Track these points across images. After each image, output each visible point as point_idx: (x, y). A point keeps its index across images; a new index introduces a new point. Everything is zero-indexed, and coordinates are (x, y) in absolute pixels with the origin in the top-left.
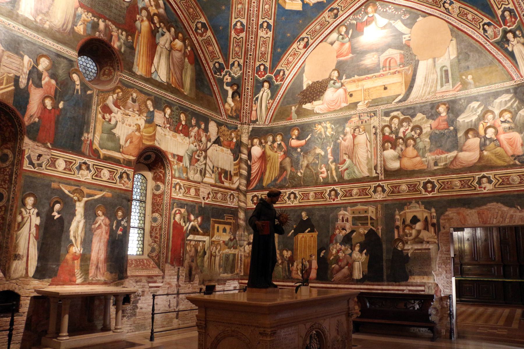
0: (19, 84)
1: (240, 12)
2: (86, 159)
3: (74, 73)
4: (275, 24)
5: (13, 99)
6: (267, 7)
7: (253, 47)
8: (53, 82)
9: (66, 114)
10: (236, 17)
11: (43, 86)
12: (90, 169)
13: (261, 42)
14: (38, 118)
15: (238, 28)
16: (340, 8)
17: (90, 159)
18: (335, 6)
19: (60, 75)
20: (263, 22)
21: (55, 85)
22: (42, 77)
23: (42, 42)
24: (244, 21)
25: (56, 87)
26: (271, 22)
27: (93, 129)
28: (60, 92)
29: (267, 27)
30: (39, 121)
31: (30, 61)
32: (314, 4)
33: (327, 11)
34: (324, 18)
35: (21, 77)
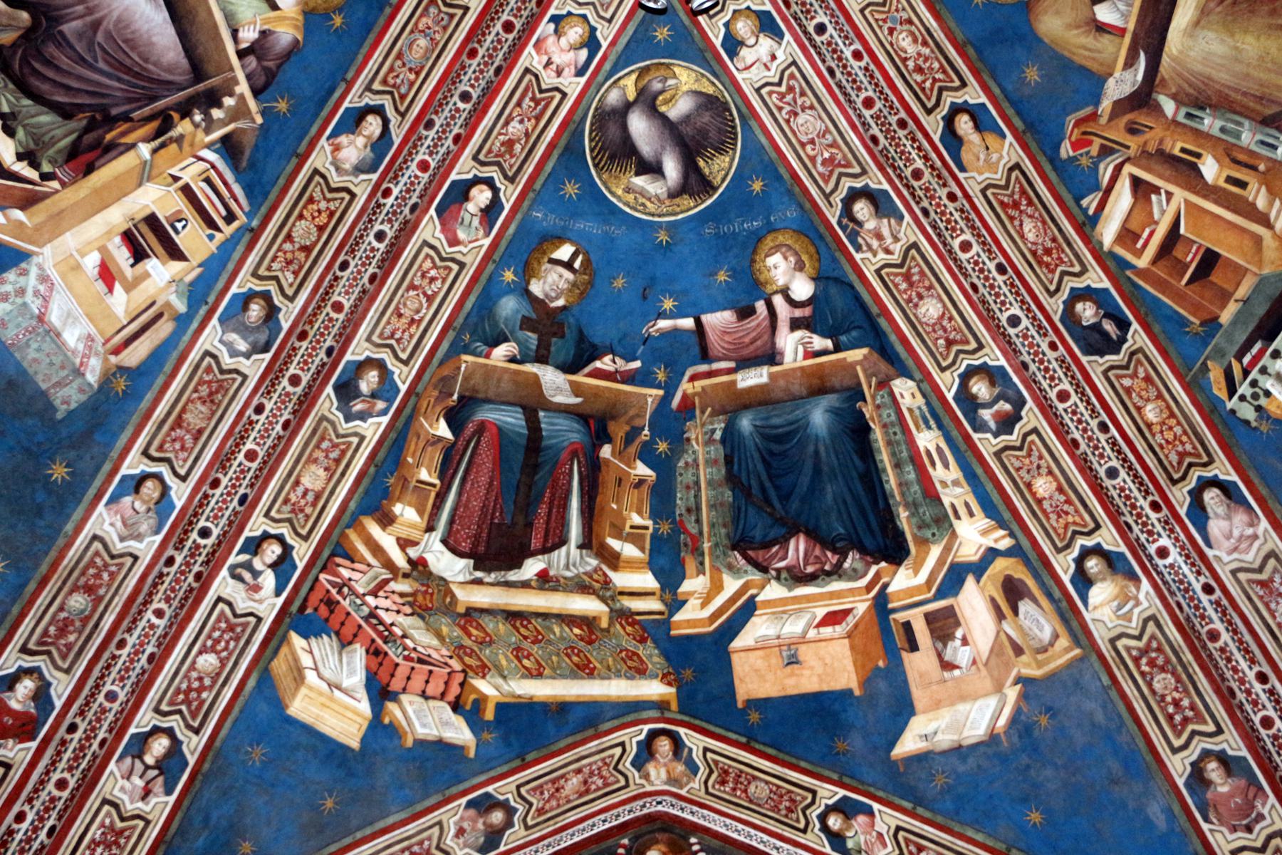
1: (63, 631)
4: (206, 766)
6: (208, 662)
7: (43, 835)
10: (31, 646)
13: (95, 832)
15: (14, 705)
16: (521, 809)
18: (504, 789)
20: (156, 730)
24: (61, 688)
26: (192, 746)
29: (160, 765)
32: (420, 743)
33: (464, 801)
34: (436, 830)
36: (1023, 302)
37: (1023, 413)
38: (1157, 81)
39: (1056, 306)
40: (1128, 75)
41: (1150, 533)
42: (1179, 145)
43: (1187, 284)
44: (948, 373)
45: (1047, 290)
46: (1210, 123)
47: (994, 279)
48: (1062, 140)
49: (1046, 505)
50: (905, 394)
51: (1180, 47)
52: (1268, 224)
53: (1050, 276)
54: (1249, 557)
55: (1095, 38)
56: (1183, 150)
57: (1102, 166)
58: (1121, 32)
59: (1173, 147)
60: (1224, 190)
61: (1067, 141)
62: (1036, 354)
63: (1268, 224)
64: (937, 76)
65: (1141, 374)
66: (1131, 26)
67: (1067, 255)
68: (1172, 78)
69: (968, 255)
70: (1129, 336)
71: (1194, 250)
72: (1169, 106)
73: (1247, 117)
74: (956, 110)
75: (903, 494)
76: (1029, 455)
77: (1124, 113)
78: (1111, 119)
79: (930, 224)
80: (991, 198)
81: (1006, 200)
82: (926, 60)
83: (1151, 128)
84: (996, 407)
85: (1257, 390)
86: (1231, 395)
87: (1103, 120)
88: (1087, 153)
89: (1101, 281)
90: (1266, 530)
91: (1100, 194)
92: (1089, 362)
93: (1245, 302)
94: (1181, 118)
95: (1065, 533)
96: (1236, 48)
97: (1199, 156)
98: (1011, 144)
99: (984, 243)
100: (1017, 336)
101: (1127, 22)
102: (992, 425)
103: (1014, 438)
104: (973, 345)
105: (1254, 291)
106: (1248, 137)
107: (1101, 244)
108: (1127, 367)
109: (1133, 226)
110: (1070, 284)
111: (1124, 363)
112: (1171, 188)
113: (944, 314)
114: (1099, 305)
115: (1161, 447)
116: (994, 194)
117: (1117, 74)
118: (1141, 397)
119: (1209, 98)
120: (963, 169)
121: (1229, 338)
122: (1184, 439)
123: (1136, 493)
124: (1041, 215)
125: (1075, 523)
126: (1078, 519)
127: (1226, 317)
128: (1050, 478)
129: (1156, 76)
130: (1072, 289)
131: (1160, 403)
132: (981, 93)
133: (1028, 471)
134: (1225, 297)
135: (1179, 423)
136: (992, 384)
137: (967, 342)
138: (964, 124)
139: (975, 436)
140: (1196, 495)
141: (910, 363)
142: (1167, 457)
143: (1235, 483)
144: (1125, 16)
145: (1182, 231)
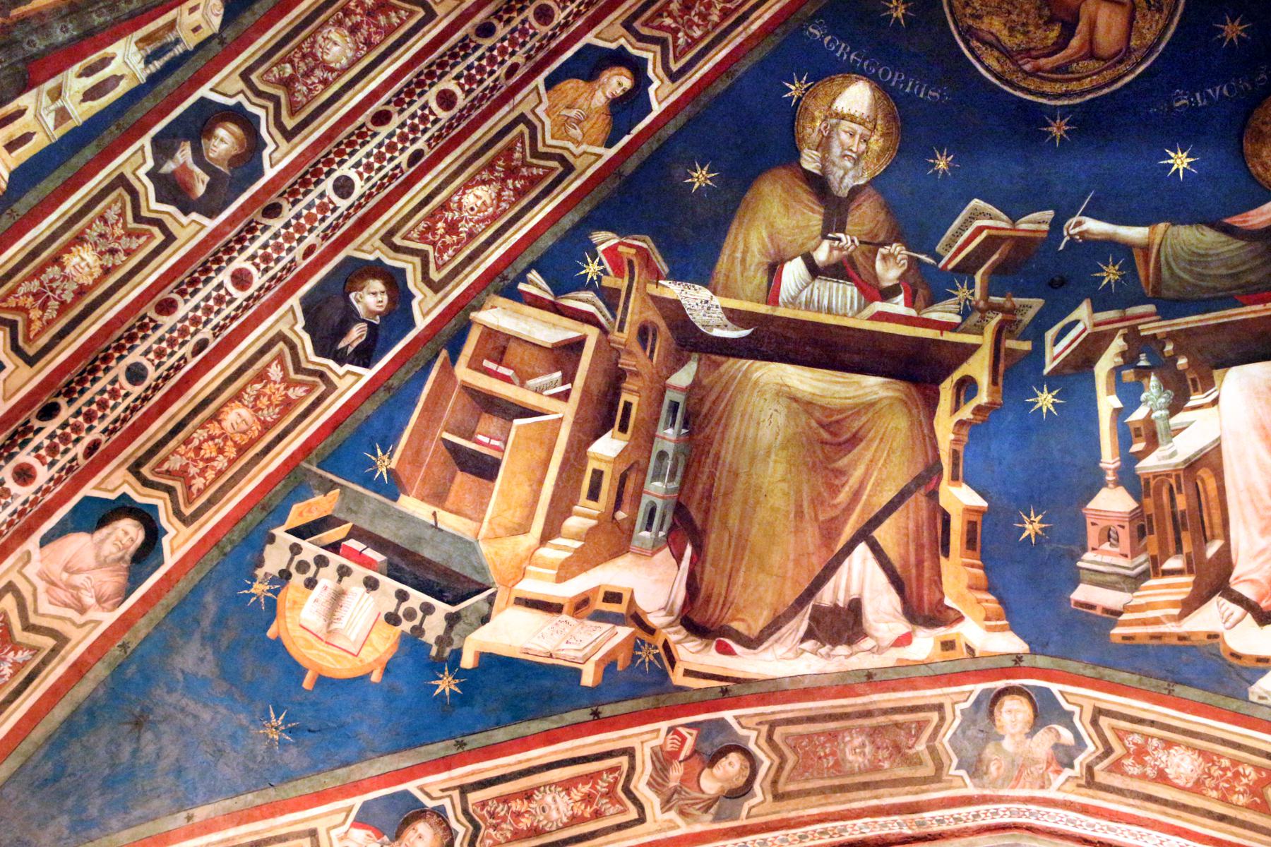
36: (370, 196)
37: (194, 216)
38: (713, 357)
39: (368, 248)
40: (718, 316)
41: (53, 450)
42: (634, 400)
43: (444, 440)
44: (241, 85)
45: (391, 233)
46: (668, 437)
47: (403, 150)
48: (619, 234)
49: (53, 271)
50: (197, 15)
51: (762, 381)
52: (545, 539)
53: (415, 235)
54: (45, 607)
55: (760, 264)
56: (628, 406)
57: (590, 295)
58: (772, 296)
59: (631, 391)
60: (583, 471)
61: (616, 241)
62: (299, 228)
63: (545, 539)
64: (680, 35)
65: (294, 393)
66: (781, 312)
67: (453, 257)
68: (721, 376)
69: (434, 105)
70: (348, 367)
71: (494, 442)
72: (683, 377)
73: (682, 484)
74: (637, 68)
75: (24, 20)
76: (130, 234)
77: (664, 318)
78: (654, 298)
79: (466, 37)
80: (515, 132)
81: (517, 155)
82: (704, 17)
83: (651, 357)
84: (197, 170)
85: (313, 568)
86: (296, 532)
87: (652, 289)
88: (604, 271)
89: (425, 315)
90: (98, 623)
91: (549, 297)
92: (292, 309)
93: (435, 527)
94: (670, 396)
95: (9, 309)
96: (768, 453)
97: (623, 428)
98: (599, 156)
99: (450, 127)
100: (322, 195)
101: (786, 306)
102: (169, 167)
103: (152, 205)
104: (290, 124)
105: (453, 536)
106: (657, 490)
107: (479, 308)
108: (298, 369)
109: (514, 351)
110: (411, 267)
111: (304, 365)
112: (575, 396)
113: (332, 70)
114: (386, 316)
115: (187, 442)
116: (522, 134)
117: (717, 301)
118: (257, 398)
119: (701, 429)
120: (550, 83)
121: (386, 513)
122: (210, 475)
123: (112, 416)
124: (505, 211)
125: (29, 323)
126: (36, 326)
127: (412, 505)
128: (97, 272)
129: (721, 354)
130: (402, 272)
131: (257, 427)
132: (665, 105)
133: (101, 236)
134: (438, 497)
135: (231, 462)
136: (235, 161)
137: (293, 114)
138: (617, 82)
139: (146, 141)
140: (123, 508)
141: (248, 19)
142: (174, 452)
143: (162, 563)
144: (793, 302)
145: (518, 422)
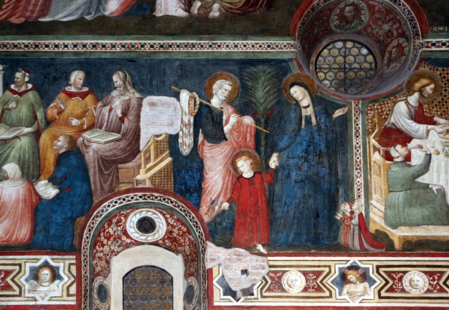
0: (178, 149)
2: (353, 260)
3: (292, 85)
5: (173, 179)
8: (248, 120)
9: (288, 176)
11: (227, 136)
12: (371, 278)
14: (228, 201)
17: (365, 255)
19: (262, 101)
21: (254, 125)
22: (222, 120)
23: (210, 50)
25: (256, 129)
27: (362, 190)
28: (266, 133)
30: (230, 207)
31: (191, 97)
35: (181, 134)
